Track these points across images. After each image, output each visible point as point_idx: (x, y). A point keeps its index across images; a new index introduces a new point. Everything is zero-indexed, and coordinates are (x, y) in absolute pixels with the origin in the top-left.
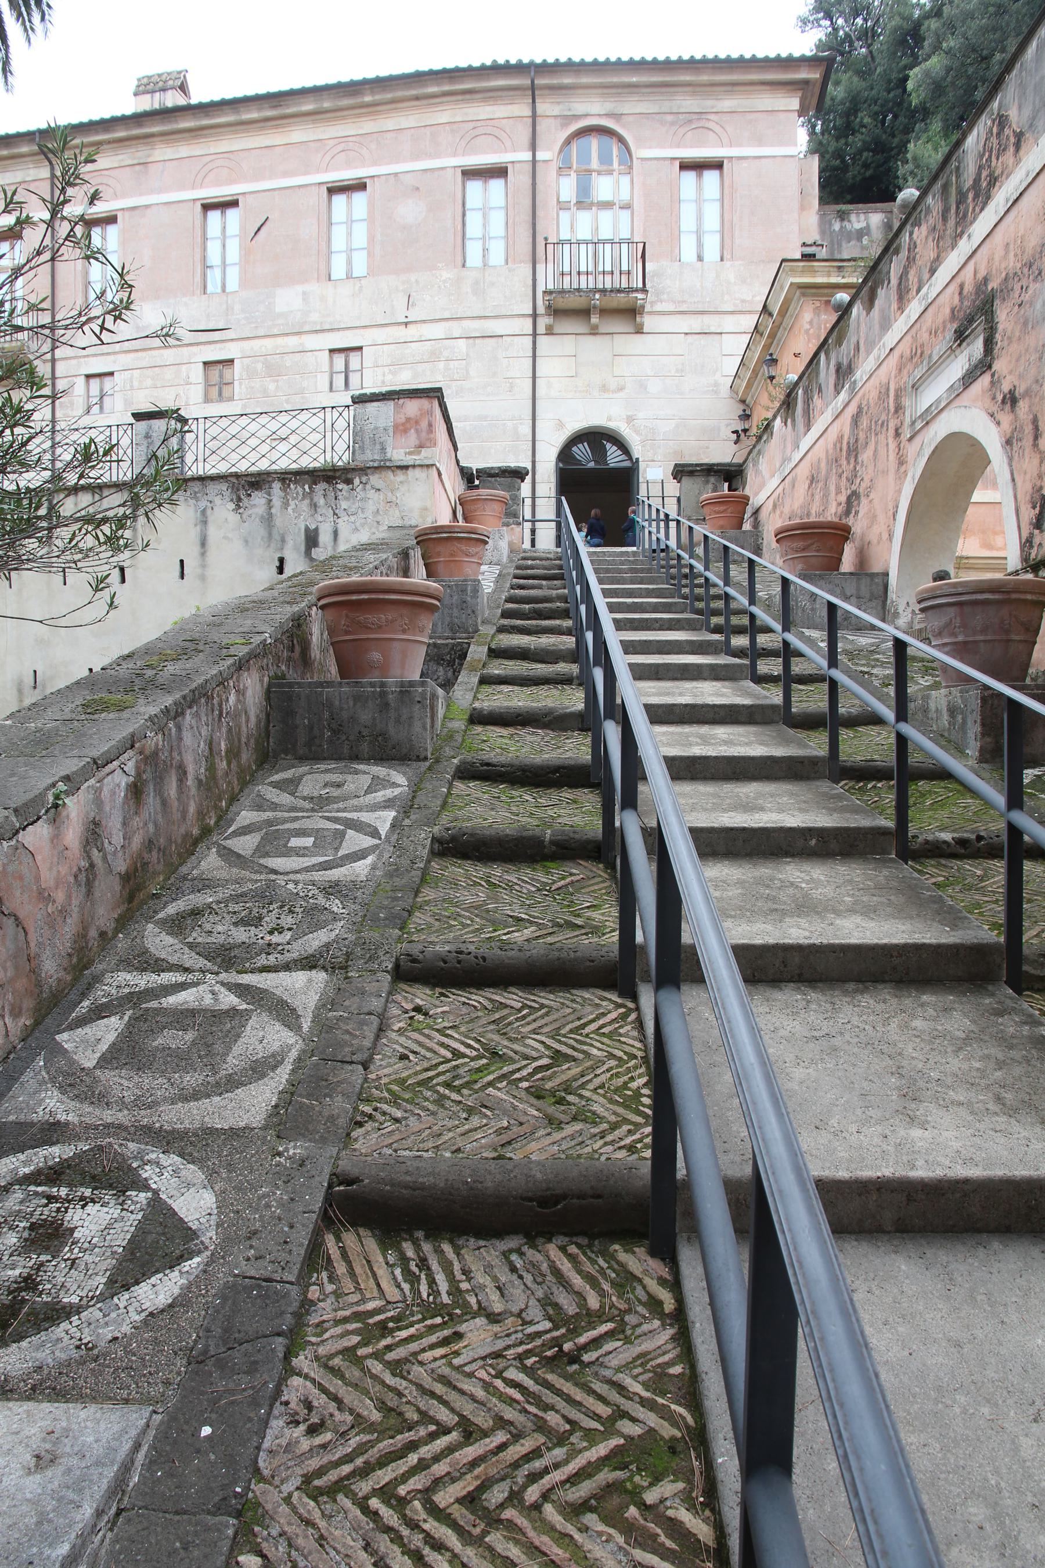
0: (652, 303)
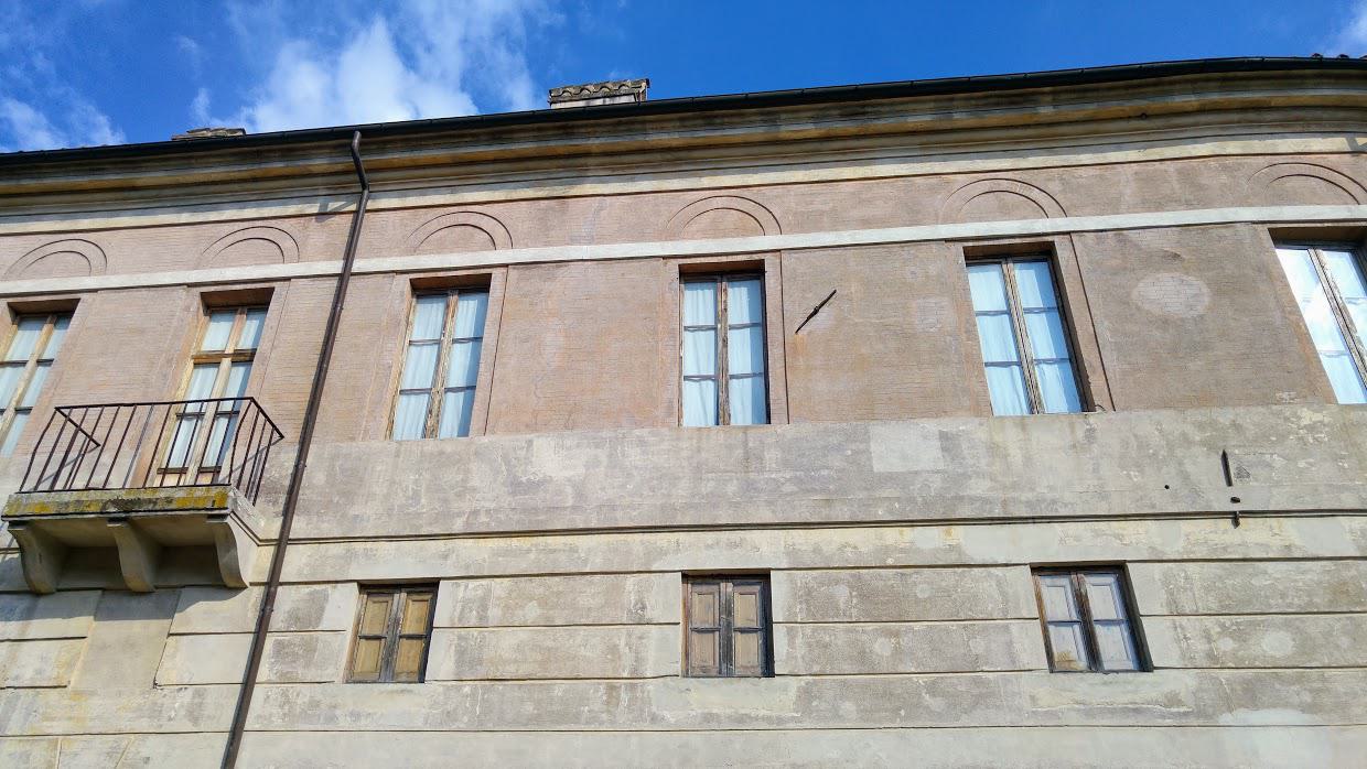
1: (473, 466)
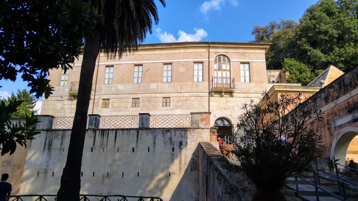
0: (236, 91)
1: (112, 88)
